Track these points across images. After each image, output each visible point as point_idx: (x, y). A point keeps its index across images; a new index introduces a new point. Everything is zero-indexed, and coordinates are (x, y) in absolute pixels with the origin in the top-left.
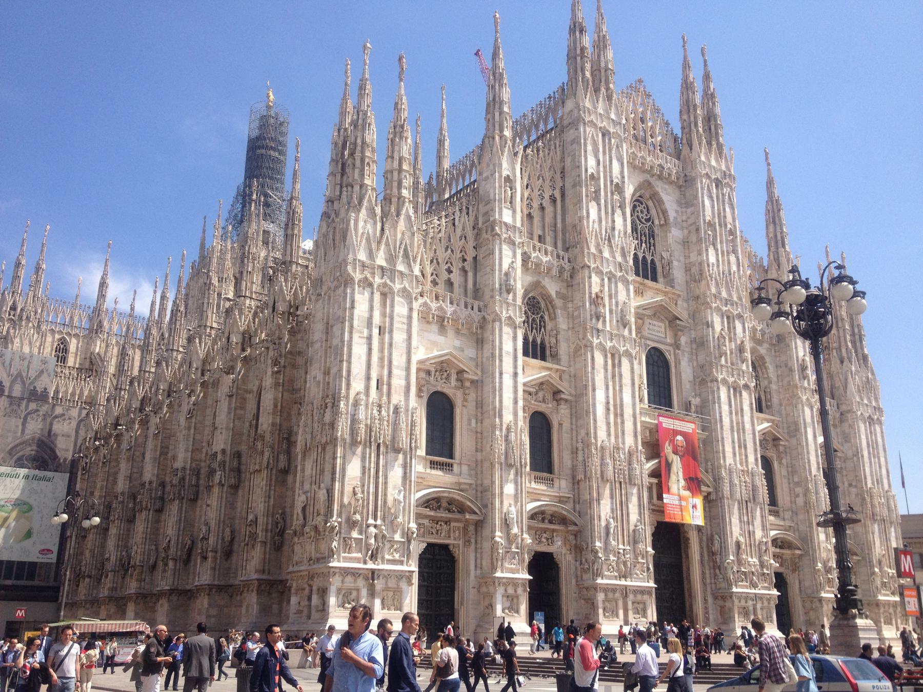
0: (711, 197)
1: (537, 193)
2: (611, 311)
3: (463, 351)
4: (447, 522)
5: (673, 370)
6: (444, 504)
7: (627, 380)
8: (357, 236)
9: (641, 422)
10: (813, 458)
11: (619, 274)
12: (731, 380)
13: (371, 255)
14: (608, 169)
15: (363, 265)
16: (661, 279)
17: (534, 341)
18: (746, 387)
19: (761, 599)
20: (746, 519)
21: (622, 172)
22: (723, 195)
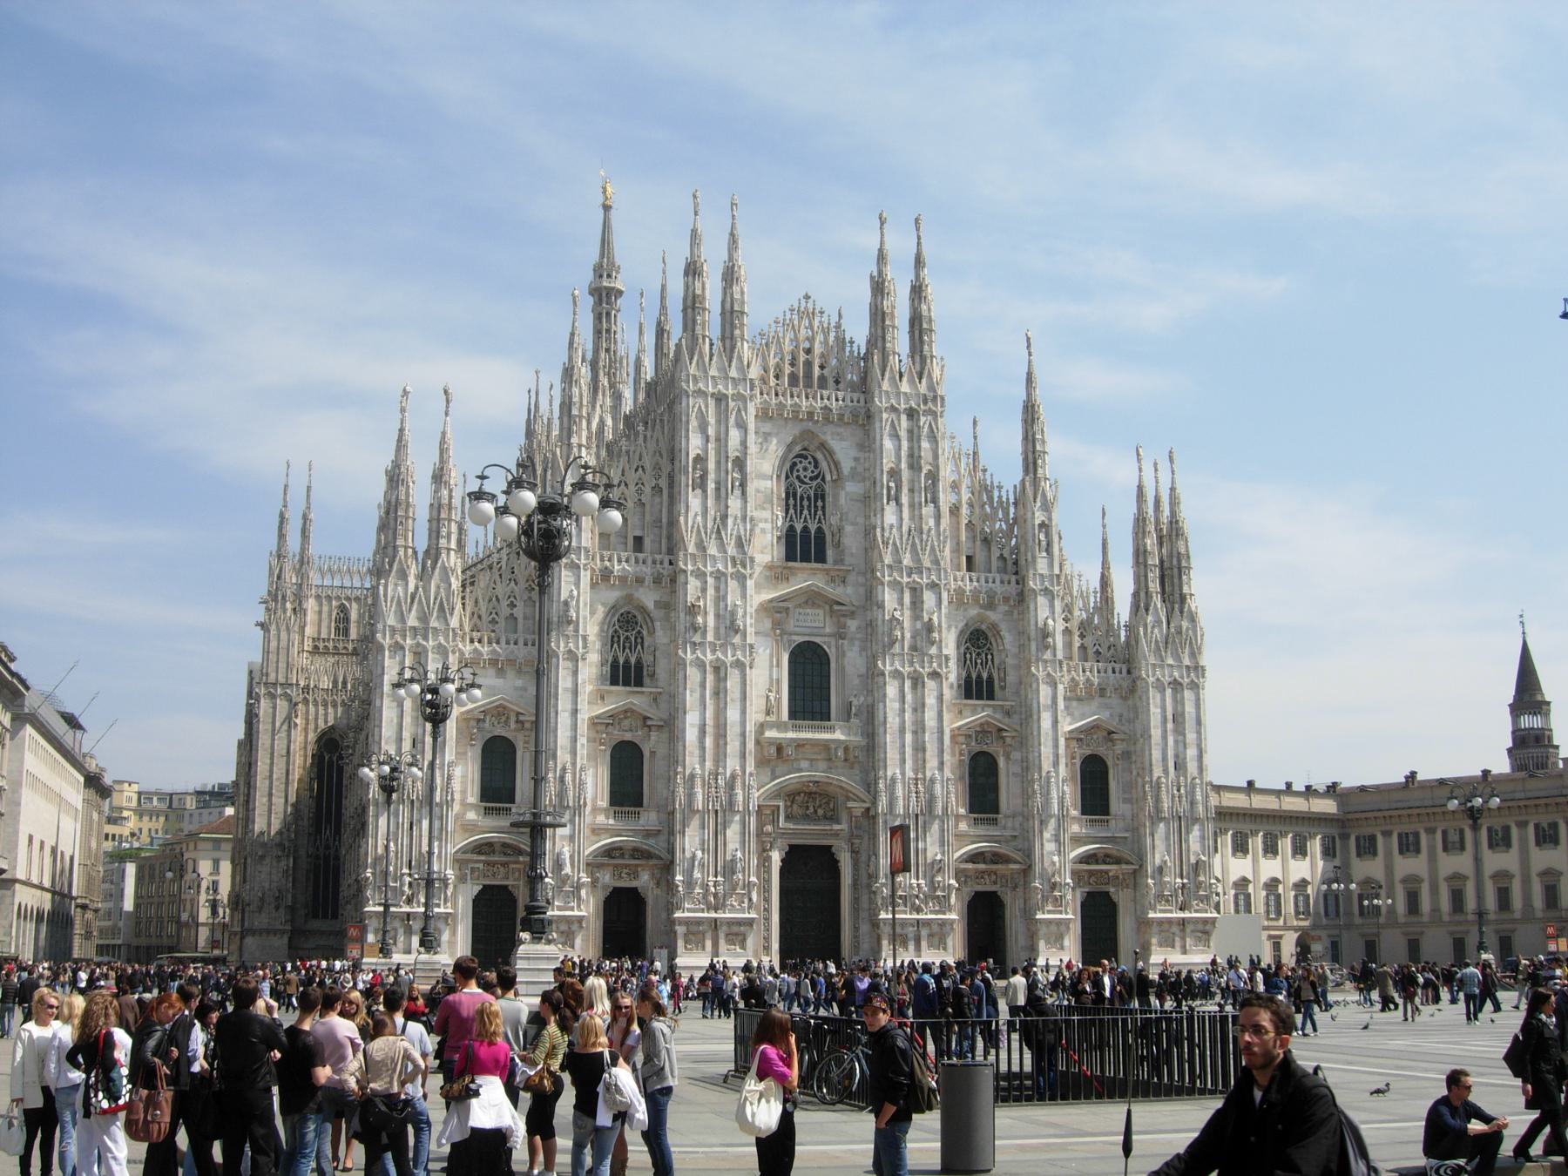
0: (895, 436)
1: (632, 488)
2: (717, 616)
4: (504, 865)
5: (833, 665)
6: (497, 848)
7: (737, 695)
9: (758, 742)
10: (1046, 751)
11: (730, 570)
13: (403, 620)
14: (722, 441)
15: (393, 630)
16: (830, 553)
17: (627, 661)
18: (935, 675)
21: (744, 443)
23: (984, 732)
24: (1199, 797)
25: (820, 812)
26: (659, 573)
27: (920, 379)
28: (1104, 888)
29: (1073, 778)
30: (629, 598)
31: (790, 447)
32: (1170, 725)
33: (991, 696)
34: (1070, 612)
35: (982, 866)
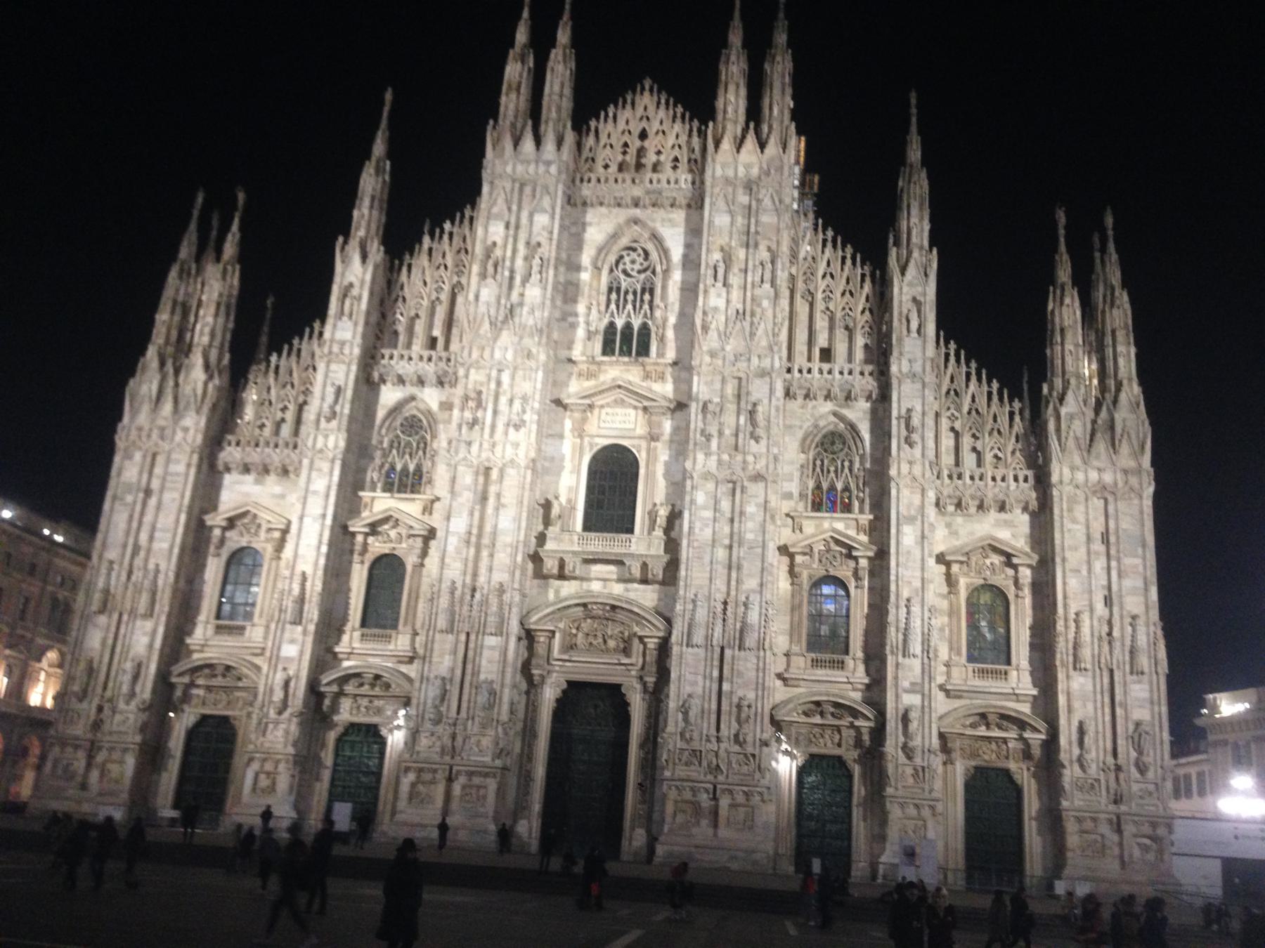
3: (283, 496)
5: (642, 471)
8: (131, 401)
12: (725, 474)
17: (405, 469)
18: (758, 477)
19: (731, 792)
20: (716, 673)
22: (758, 201)
23: (828, 550)
24: (1142, 640)
25: (612, 644)
26: (446, 373)
27: (762, 145)
28: (1000, 764)
29: (953, 612)
30: (413, 398)
31: (614, 237)
32: (1098, 547)
33: (847, 508)
34: (959, 409)
35: (817, 720)
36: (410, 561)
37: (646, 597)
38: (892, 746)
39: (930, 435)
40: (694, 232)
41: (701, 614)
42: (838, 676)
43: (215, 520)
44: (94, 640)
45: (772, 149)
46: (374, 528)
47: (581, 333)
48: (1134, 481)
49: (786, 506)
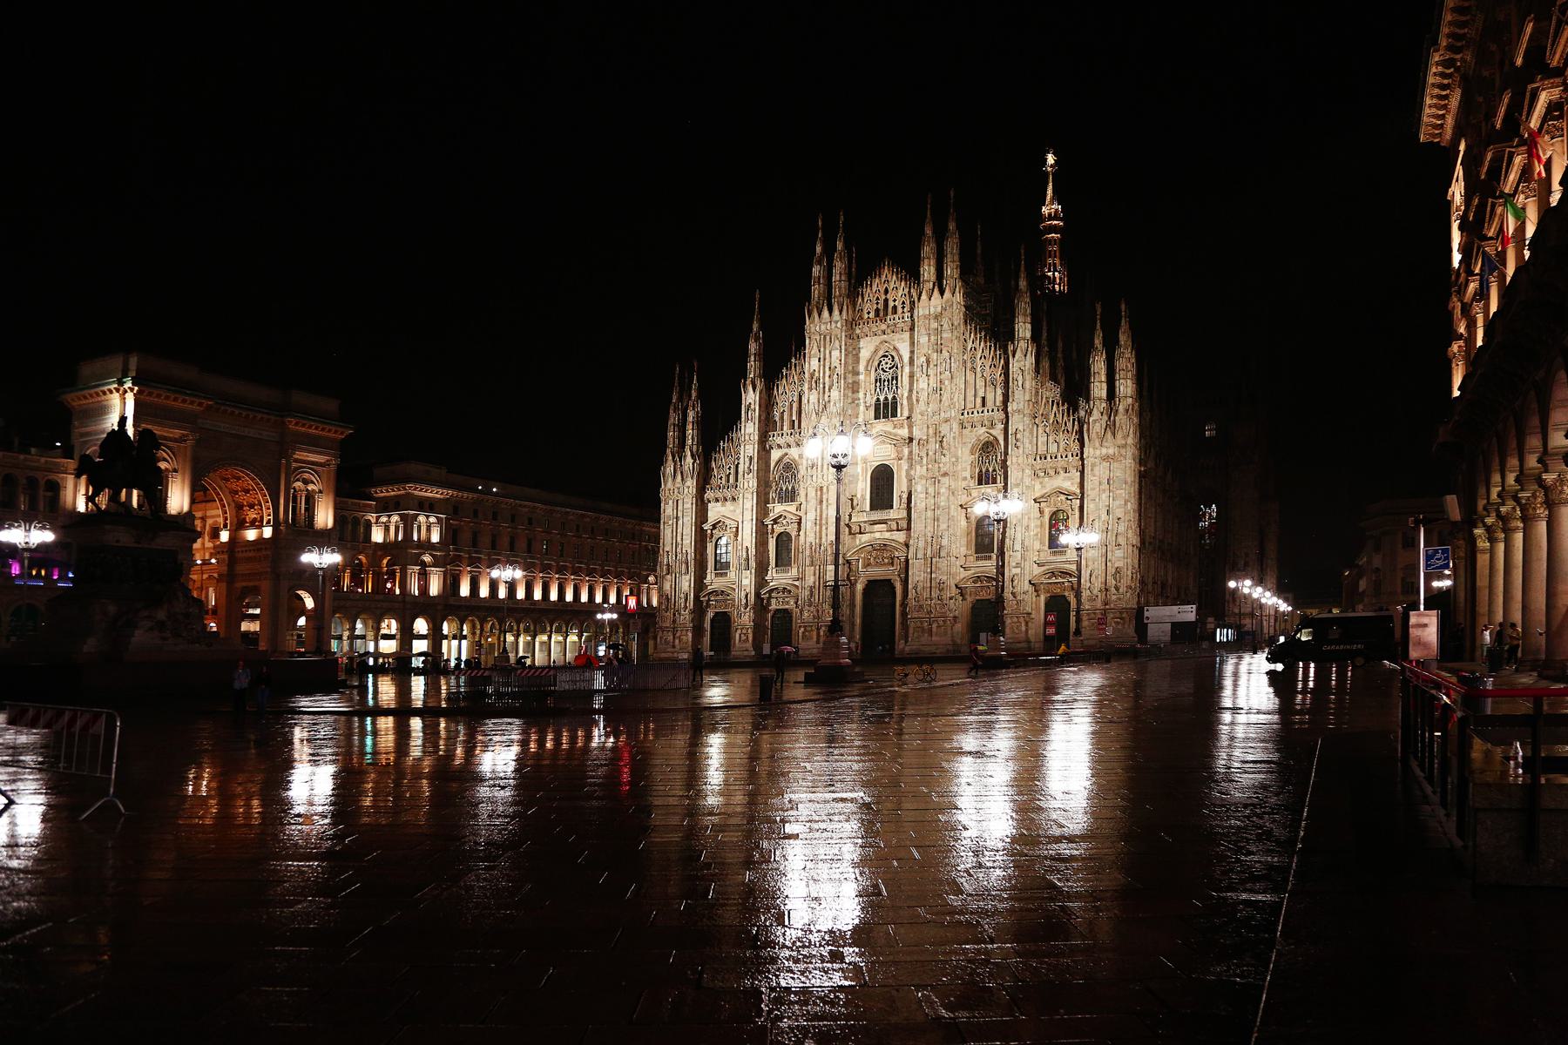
18: (945, 474)
27: (942, 293)
31: (876, 351)
33: (994, 482)
36: (793, 534)
37: (901, 537)
38: (1007, 595)
39: (1026, 441)
40: (912, 344)
41: (921, 544)
42: (988, 563)
43: (706, 527)
44: (667, 586)
45: (947, 294)
46: (775, 521)
47: (862, 408)
48: (1123, 451)
49: (964, 484)
